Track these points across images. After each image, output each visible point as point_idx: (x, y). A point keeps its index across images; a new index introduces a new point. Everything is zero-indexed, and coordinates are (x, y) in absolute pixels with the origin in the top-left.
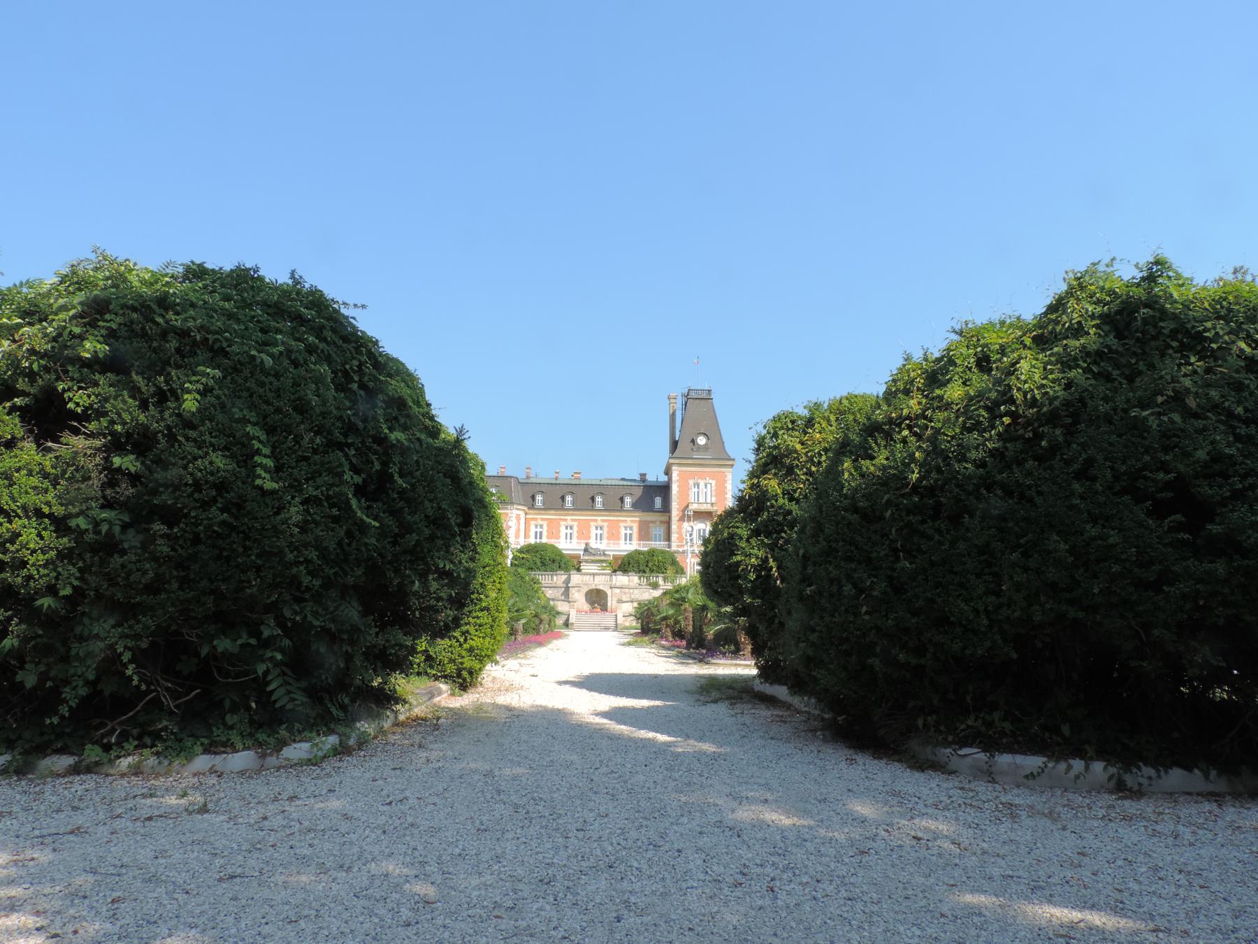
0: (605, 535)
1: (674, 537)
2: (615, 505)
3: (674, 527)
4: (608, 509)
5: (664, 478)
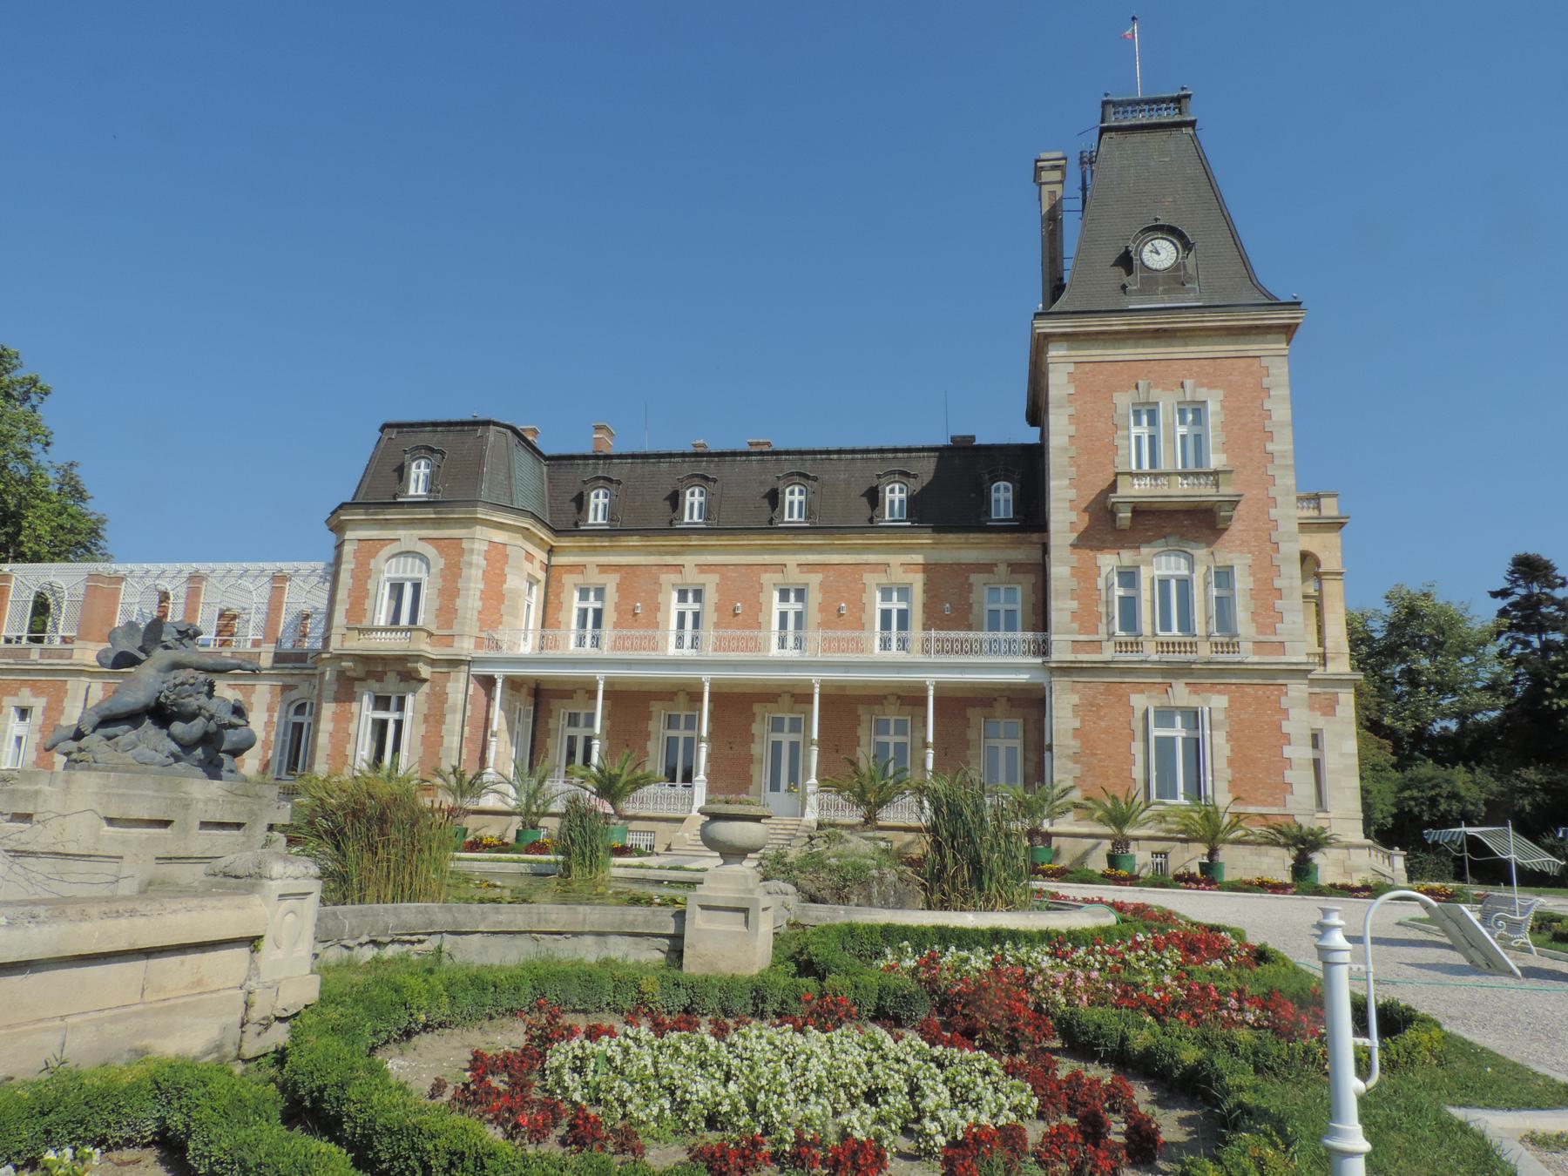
0: (813, 616)
1: (1061, 609)
2: (848, 512)
3: (1060, 571)
4: (819, 526)
5: (1031, 436)
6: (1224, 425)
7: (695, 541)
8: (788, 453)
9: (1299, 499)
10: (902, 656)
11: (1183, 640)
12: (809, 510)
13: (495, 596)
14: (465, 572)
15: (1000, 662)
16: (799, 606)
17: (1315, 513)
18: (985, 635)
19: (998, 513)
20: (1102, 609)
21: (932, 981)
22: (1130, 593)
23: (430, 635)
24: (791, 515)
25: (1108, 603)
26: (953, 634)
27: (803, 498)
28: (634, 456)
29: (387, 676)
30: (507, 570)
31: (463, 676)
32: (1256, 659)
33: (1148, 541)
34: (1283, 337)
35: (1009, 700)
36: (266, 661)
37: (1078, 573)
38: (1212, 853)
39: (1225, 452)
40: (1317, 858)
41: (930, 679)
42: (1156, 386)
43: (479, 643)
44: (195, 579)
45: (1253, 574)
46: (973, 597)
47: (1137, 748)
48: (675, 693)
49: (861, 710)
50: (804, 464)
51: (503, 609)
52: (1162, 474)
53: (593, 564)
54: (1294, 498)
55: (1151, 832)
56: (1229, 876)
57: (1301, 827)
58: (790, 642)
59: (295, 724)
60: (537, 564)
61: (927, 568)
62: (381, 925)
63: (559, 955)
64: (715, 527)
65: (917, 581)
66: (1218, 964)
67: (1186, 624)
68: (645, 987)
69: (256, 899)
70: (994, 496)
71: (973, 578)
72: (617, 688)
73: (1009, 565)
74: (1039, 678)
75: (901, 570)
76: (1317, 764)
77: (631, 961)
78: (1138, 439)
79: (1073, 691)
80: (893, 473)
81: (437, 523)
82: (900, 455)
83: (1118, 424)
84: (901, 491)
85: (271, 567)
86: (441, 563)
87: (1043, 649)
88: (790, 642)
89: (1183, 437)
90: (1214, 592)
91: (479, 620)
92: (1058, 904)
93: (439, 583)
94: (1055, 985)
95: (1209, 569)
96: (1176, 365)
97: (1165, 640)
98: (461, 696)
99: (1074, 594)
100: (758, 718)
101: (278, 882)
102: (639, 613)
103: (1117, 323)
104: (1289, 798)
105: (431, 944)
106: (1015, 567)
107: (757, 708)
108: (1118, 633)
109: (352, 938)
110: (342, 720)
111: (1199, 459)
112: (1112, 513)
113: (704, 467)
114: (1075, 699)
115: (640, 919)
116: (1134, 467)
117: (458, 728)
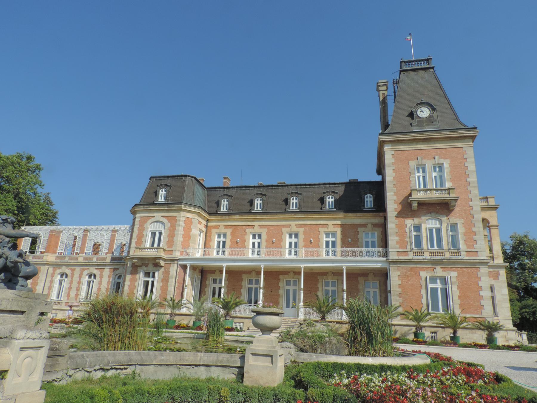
1: (392, 240)
2: (313, 207)
3: (392, 226)
4: (304, 211)
5: (379, 178)
6: (451, 172)
7: (258, 217)
8: (291, 185)
9: (480, 199)
10: (334, 258)
11: (439, 251)
12: (299, 205)
13: (187, 236)
14: (177, 228)
15: (370, 260)
16: (296, 240)
17: (486, 204)
18: (364, 250)
19: (367, 206)
20: (408, 240)
21: (357, 391)
22: (418, 234)
23: (164, 250)
24: (293, 207)
25: (410, 237)
26: (352, 249)
27: (297, 201)
28: (237, 187)
29: (150, 265)
30: (192, 227)
31: (176, 265)
32: (467, 258)
33: (424, 215)
34: (471, 140)
35: (374, 274)
36: (108, 260)
37: (398, 226)
38: (455, 332)
39: (451, 182)
40: (496, 335)
41: (344, 266)
42: (425, 158)
43: (182, 253)
44: (86, 231)
45: (464, 226)
46: (359, 236)
47: (423, 291)
48: (251, 272)
49: (319, 277)
50: (296, 189)
51: (190, 241)
52: (428, 190)
53: (222, 225)
54: (478, 198)
55: (430, 324)
56: (462, 341)
57: (489, 322)
58: (293, 253)
59: (117, 283)
60: (203, 225)
61: (342, 226)
62: (106, 361)
63: (189, 375)
64: (265, 212)
65: (339, 231)
66: (480, 382)
67: (440, 245)
68: (223, 394)
69: (7, 350)
70: (366, 199)
71: (359, 229)
72: (230, 270)
73: (372, 224)
74: (385, 265)
75: (332, 226)
76: (493, 298)
77: (221, 378)
78: (419, 178)
79: (398, 270)
80: (329, 192)
81: (168, 211)
82: (331, 186)
83: (410, 173)
84: (332, 198)
85: (111, 227)
86: (169, 225)
87: (386, 255)
88: (293, 253)
89: (435, 177)
90: (451, 233)
91: (182, 245)
92: (404, 354)
93: (168, 232)
94: (417, 395)
95: (447, 224)
96: (432, 151)
97: (432, 251)
98: (175, 272)
99: (397, 234)
100: (281, 280)
101: (21, 341)
102: (239, 243)
103: (409, 137)
104: (483, 311)
105: (130, 370)
106: (374, 225)
107: (281, 277)
108: (414, 248)
109: (90, 367)
110: (133, 281)
111: (442, 185)
112: (410, 204)
113: (262, 191)
114: (399, 273)
115: (225, 359)
116: (417, 187)
117: (173, 284)
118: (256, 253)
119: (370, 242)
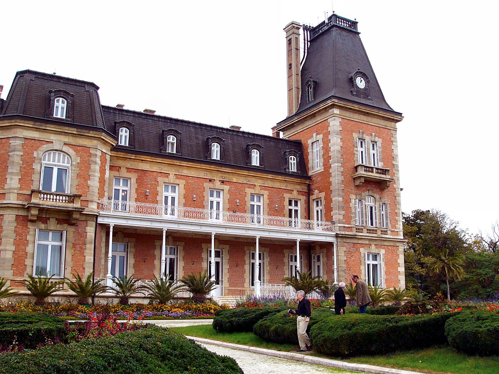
4: (224, 163)
32: (391, 237)
118: (169, 211)
119: (293, 211)
